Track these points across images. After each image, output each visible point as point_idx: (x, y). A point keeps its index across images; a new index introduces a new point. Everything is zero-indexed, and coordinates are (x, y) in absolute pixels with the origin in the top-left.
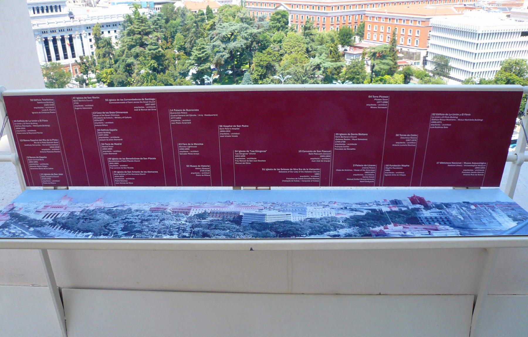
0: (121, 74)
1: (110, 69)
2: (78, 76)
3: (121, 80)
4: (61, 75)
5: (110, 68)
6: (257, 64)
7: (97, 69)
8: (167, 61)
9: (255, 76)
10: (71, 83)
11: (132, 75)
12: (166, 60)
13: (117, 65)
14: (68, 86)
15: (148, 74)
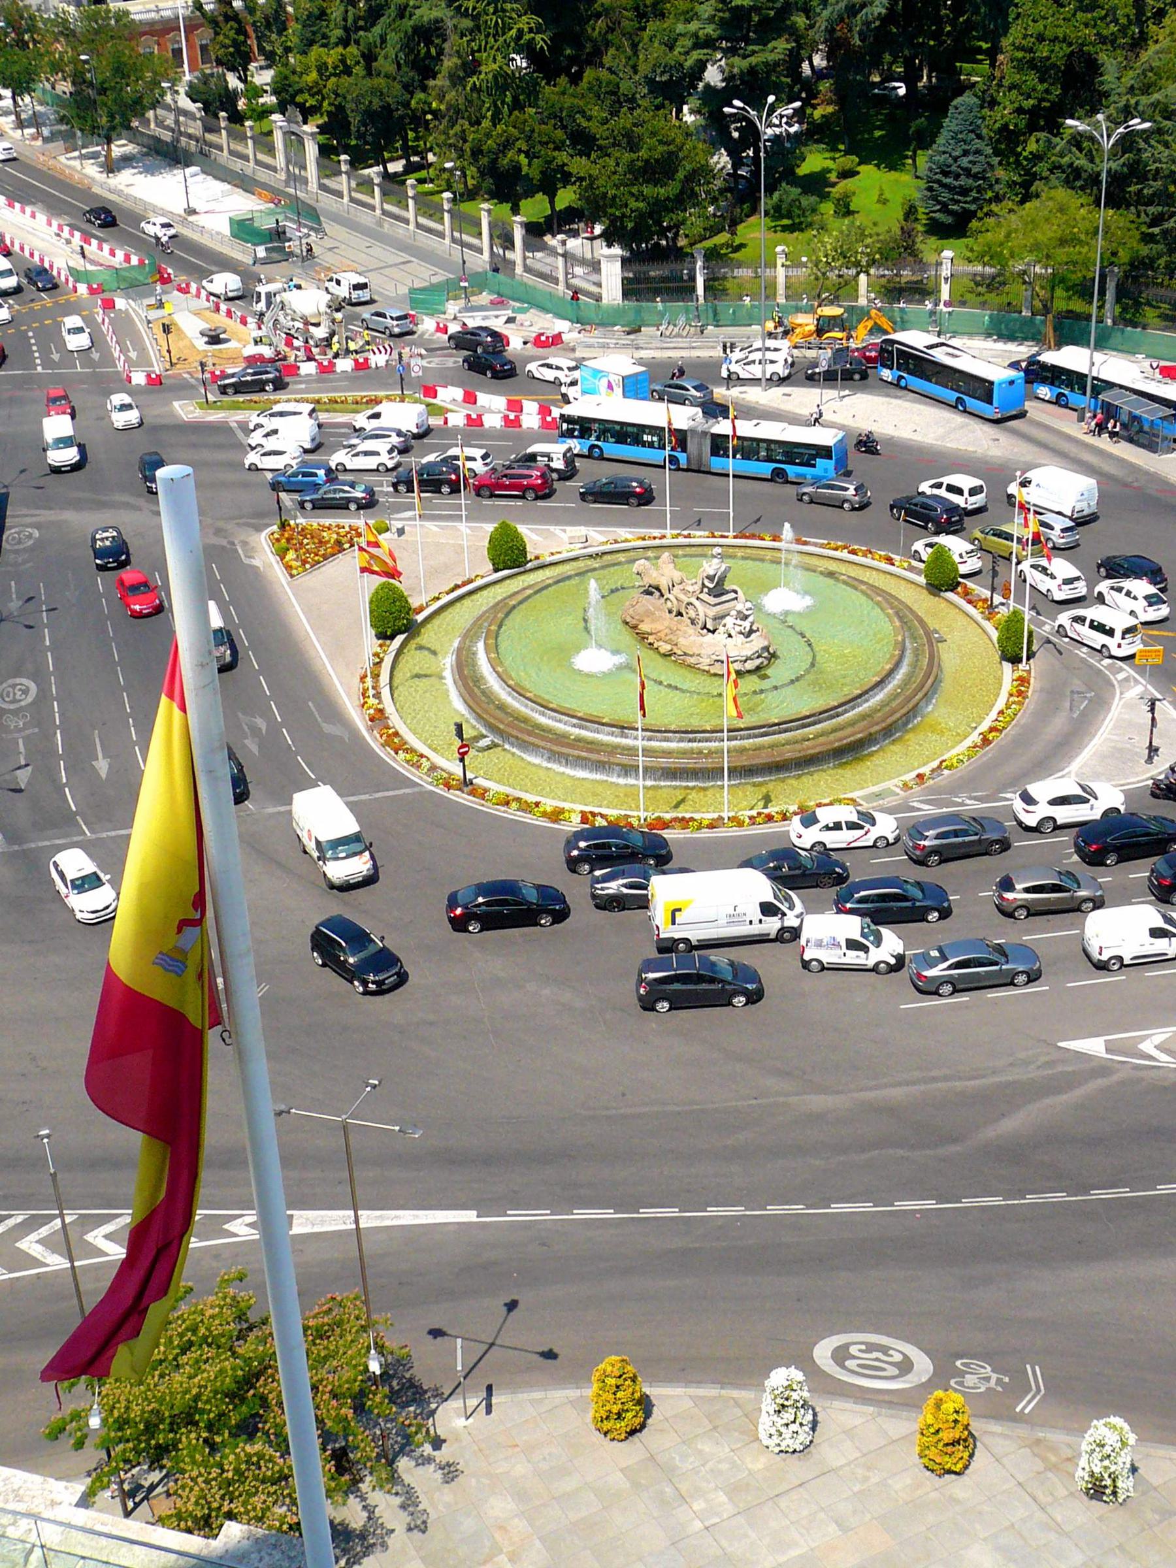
0: (387, 76)
1: (340, 49)
2: (205, 79)
3: (376, 104)
4: (121, 71)
5: (345, 42)
6: (1020, 54)
7: (288, 50)
8: (601, 24)
9: (1004, 113)
10: (168, 108)
11: (431, 83)
12: (598, 16)
13: (377, 30)
14: (160, 123)
15: (503, 81)
